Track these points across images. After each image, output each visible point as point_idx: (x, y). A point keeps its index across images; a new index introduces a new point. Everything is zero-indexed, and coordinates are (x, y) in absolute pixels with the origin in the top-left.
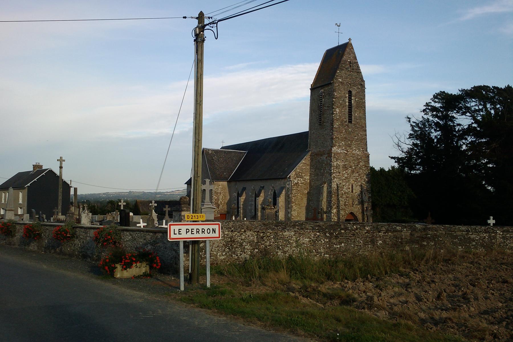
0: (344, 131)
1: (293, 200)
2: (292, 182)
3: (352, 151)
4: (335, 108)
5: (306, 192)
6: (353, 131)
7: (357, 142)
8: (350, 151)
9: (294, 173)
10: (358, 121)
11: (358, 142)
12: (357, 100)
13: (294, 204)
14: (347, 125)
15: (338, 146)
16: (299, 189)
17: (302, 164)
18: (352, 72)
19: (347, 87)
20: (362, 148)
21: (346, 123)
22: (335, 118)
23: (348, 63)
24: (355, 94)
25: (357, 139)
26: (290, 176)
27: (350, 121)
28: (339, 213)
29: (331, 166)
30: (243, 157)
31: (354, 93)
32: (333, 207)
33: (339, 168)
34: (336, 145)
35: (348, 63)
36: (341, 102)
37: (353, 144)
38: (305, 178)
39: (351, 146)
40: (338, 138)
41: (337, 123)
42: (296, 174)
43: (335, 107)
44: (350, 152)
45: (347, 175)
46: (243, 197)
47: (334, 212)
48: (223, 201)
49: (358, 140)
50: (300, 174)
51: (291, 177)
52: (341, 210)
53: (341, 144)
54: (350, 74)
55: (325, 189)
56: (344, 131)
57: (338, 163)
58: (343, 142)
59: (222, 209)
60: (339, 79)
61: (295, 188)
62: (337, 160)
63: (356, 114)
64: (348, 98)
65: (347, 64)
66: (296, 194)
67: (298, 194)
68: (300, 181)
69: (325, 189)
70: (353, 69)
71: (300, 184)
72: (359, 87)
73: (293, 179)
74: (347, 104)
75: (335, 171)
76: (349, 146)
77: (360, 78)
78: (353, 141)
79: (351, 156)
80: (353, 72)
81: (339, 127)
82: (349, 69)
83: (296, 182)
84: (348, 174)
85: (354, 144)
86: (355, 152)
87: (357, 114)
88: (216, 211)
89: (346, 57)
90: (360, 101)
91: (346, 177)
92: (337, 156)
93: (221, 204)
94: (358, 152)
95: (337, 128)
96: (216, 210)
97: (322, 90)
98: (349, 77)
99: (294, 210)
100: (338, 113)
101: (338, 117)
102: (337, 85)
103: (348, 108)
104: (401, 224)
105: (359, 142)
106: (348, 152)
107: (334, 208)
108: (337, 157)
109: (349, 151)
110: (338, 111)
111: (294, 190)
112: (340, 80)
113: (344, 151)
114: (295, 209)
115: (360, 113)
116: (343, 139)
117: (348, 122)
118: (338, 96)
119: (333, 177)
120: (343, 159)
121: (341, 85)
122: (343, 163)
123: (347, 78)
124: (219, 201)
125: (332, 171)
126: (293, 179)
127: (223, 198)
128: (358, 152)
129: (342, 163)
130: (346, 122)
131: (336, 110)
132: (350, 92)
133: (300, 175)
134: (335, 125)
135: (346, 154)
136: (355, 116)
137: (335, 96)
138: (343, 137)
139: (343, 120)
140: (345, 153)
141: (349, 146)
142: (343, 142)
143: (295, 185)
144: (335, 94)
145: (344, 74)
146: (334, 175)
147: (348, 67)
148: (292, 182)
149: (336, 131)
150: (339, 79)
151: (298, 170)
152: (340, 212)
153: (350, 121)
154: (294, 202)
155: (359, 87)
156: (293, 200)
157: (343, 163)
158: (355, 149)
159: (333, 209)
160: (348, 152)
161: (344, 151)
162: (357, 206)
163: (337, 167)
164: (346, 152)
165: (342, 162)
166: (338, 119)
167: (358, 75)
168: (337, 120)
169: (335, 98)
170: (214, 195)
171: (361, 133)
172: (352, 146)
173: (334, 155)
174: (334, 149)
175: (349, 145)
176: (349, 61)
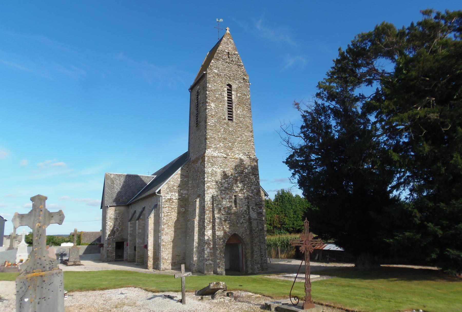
0: (222, 130)
1: (164, 221)
2: (163, 198)
3: (234, 155)
4: (208, 102)
5: (183, 210)
6: (234, 131)
7: (241, 145)
8: (232, 155)
9: (166, 186)
10: (241, 119)
11: (242, 144)
12: (238, 95)
13: (166, 225)
14: (227, 124)
15: (215, 148)
16: (173, 207)
17: (177, 176)
18: (231, 64)
19: (226, 80)
20: (248, 152)
21: (225, 121)
22: (210, 114)
23: (225, 53)
24: (236, 89)
25: (241, 141)
26: (160, 190)
27: (230, 118)
28: (215, 236)
29: (204, 173)
30: (150, 181)
31: (234, 87)
32: (207, 228)
33: (216, 176)
34: (211, 146)
35: (225, 53)
36: (217, 96)
37: (236, 146)
38: (182, 192)
39: (232, 149)
40: (214, 138)
41: (213, 120)
42: (169, 187)
43: (208, 101)
44: (231, 156)
45: (227, 185)
46: (132, 222)
47: (209, 235)
48: (119, 227)
49: (241, 142)
50: (175, 187)
51: (161, 191)
52: (218, 230)
53: (218, 146)
54: (228, 66)
55: (198, 203)
56: (222, 130)
57: (214, 169)
58: (221, 144)
59: (119, 237)
60: (214, 70)
61: (167, 206)
62: (212, 165)
63: (238, 112)
64: (226, 92)
65: (225, 55)
66: (168, 212)
67: (172, 213)
68: (175, 196)
69: (198, 203)
70: (232, 61)
71: (175, 201)
72: (242, 81)
73: (164, 194)
74: (226, 99)
75: (209, 180)
76: (231, 148)
77: (242, 72)
78: (235, 142)
79: (233, 161)
80: (232, 64)
81: (215, 126)
82: (228, 61)
83: (169, 198)
84: (229, 184)
85: (237, 147)
86: (238, 156)
87: (240, 112)
88: (111, 240)
89: (222, 46)
90: (243, 97)
91: (225, 188)
92: (213, 160)
93: (117, 231)
94: (242, 156)
95: (213, 126)
96: (111, 238)
97: (198, 87)
98: (227, 68)
99: (165, 234)
100: (213, 108)
101: (213, 113)
102: (211, 76)
103: (227, 104)
104: (166, 286)
105: (243, 145)
106: (229, 155)
107: (208, 229)
108: (212, 162)
109: (230, 154)
110: (214, 106)
111: (166, 207)
112: (216, 71)
113: (223, 155)
114: (167, 233)
115: (243, 110)
116: (221, 140)
117: (227, 119)
118: (213, 88)
119: (207, 188)
120: (221, 165)
121: (216, 77)
122: (221, 169)
123: (225, 70)
124: (115, 227)
125: (206, 179)
126: (164, 194)
127: (120, 224)
128: (242, 156)
129: (220, 169)
130: (225, 120)
131: (211, 104)
132: (229, 85)
133: (174, 188)
134: (209, 122)
135: (226, 158)
136: (237, 114)
137: (209, 89)
138: (220, 137)
139: (220, 117)
140: (223, 156)
141: (231, 148)
142: (221, 144)
143: (167, 201)
144: (209, 87)
145: (221, 65)
146: (208, 184)
147: (226, 58)
148: (163, 198)
149: (210, 130)
150: (214, 70)
151: (172, 183)
152: (215, 233)
153: (230, 118)
154: (166, 223)
155: (242, 81)
156: (164, 221)
157: (221, 169)
158: (238, 152)
159: (207, 230)
160: (229, 155)
161: (223, 155)
162: (243, 224)
163: (212, 175)
164: (226, 156)
165: (220, 168)
166: (214, 115)
167: (239, 68)
168: (212, 117)
169: (209, 91)
170: (109, 221)
171: (246, 134)
172: (234, 149)
173: (209, 159)
174: (209, 152)
175: (230, 147)
176: (227, 51)
